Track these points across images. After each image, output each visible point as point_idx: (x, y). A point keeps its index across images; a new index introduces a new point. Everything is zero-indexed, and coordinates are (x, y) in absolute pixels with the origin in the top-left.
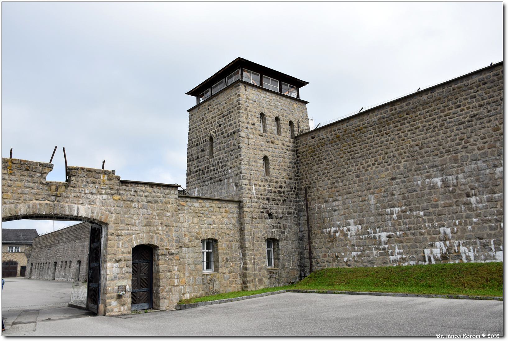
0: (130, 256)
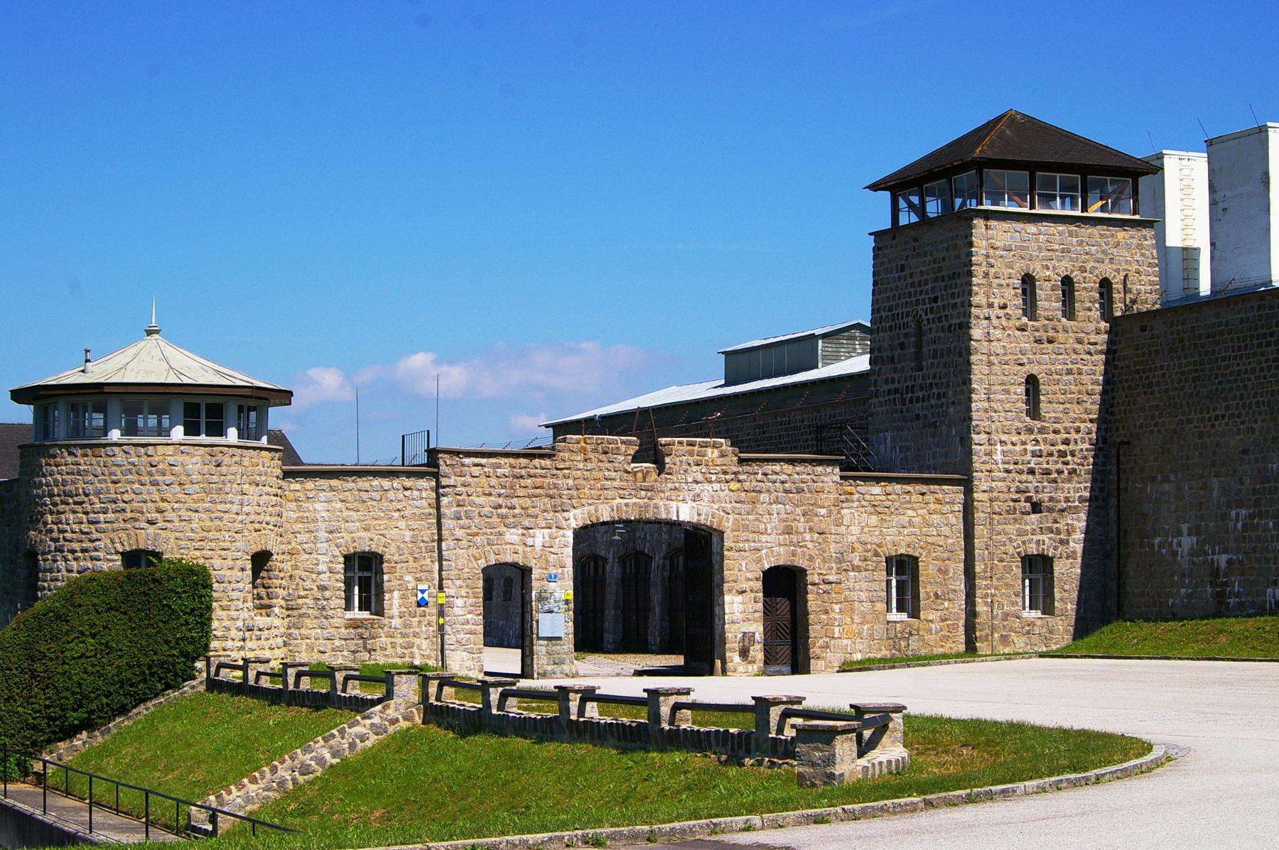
0: (759, 585)
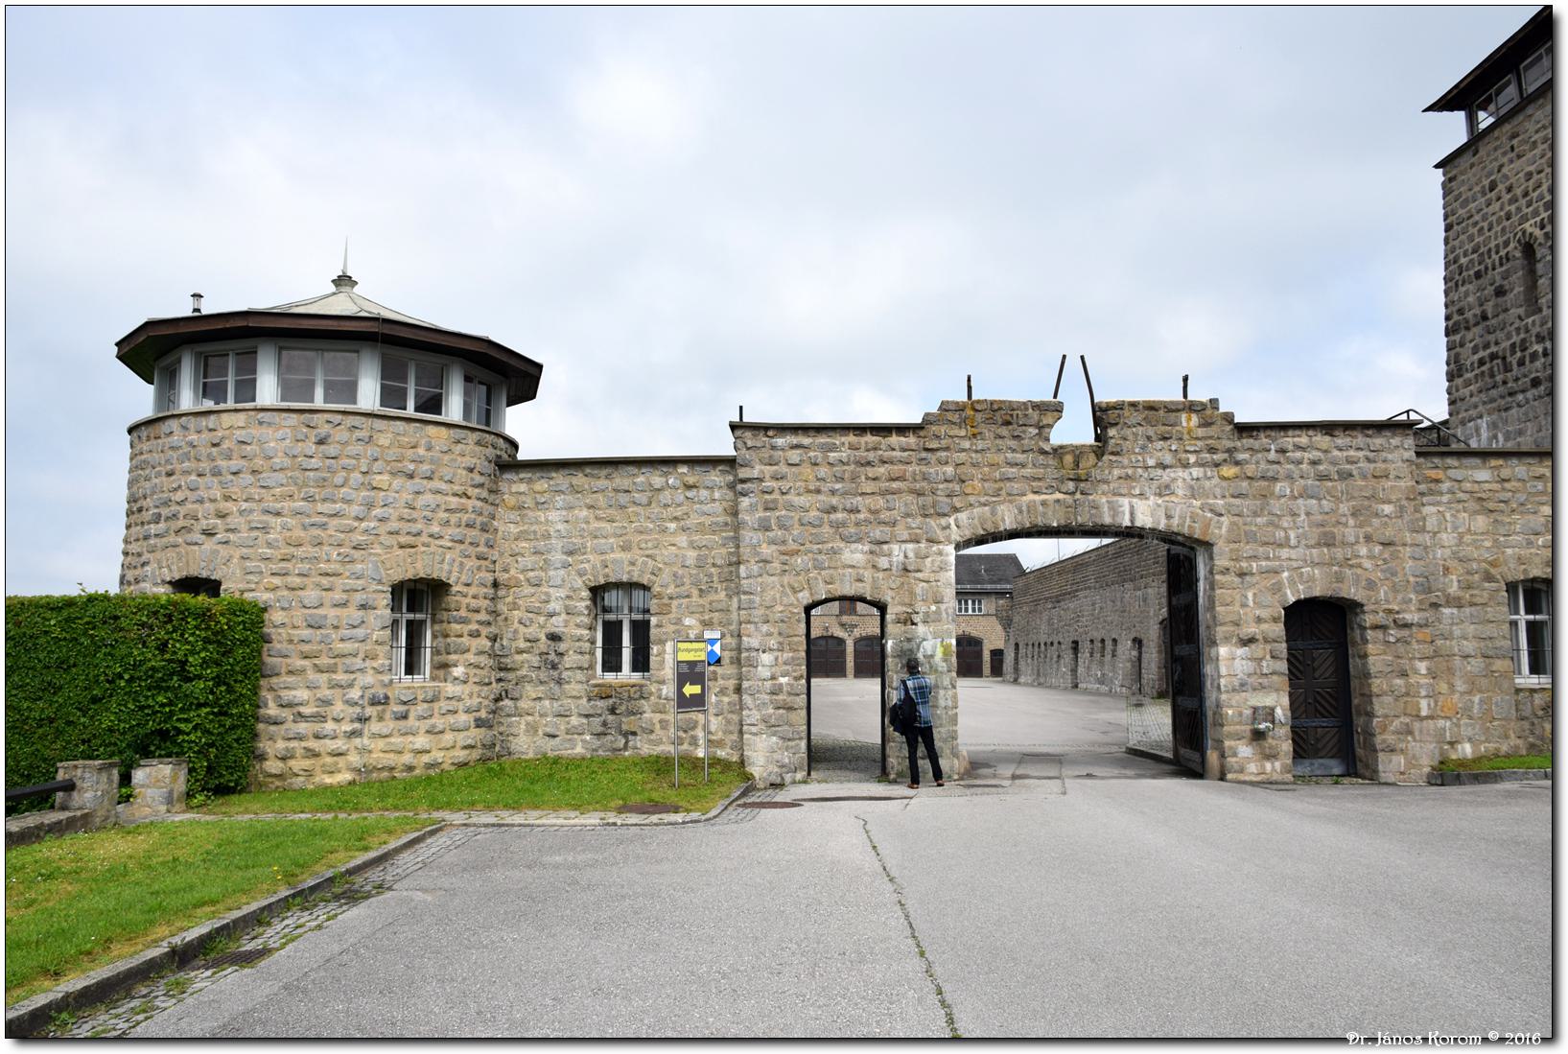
0: (1278, 630)
